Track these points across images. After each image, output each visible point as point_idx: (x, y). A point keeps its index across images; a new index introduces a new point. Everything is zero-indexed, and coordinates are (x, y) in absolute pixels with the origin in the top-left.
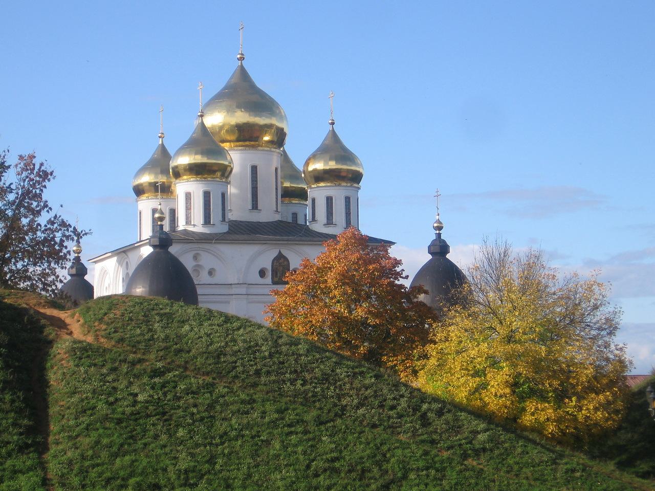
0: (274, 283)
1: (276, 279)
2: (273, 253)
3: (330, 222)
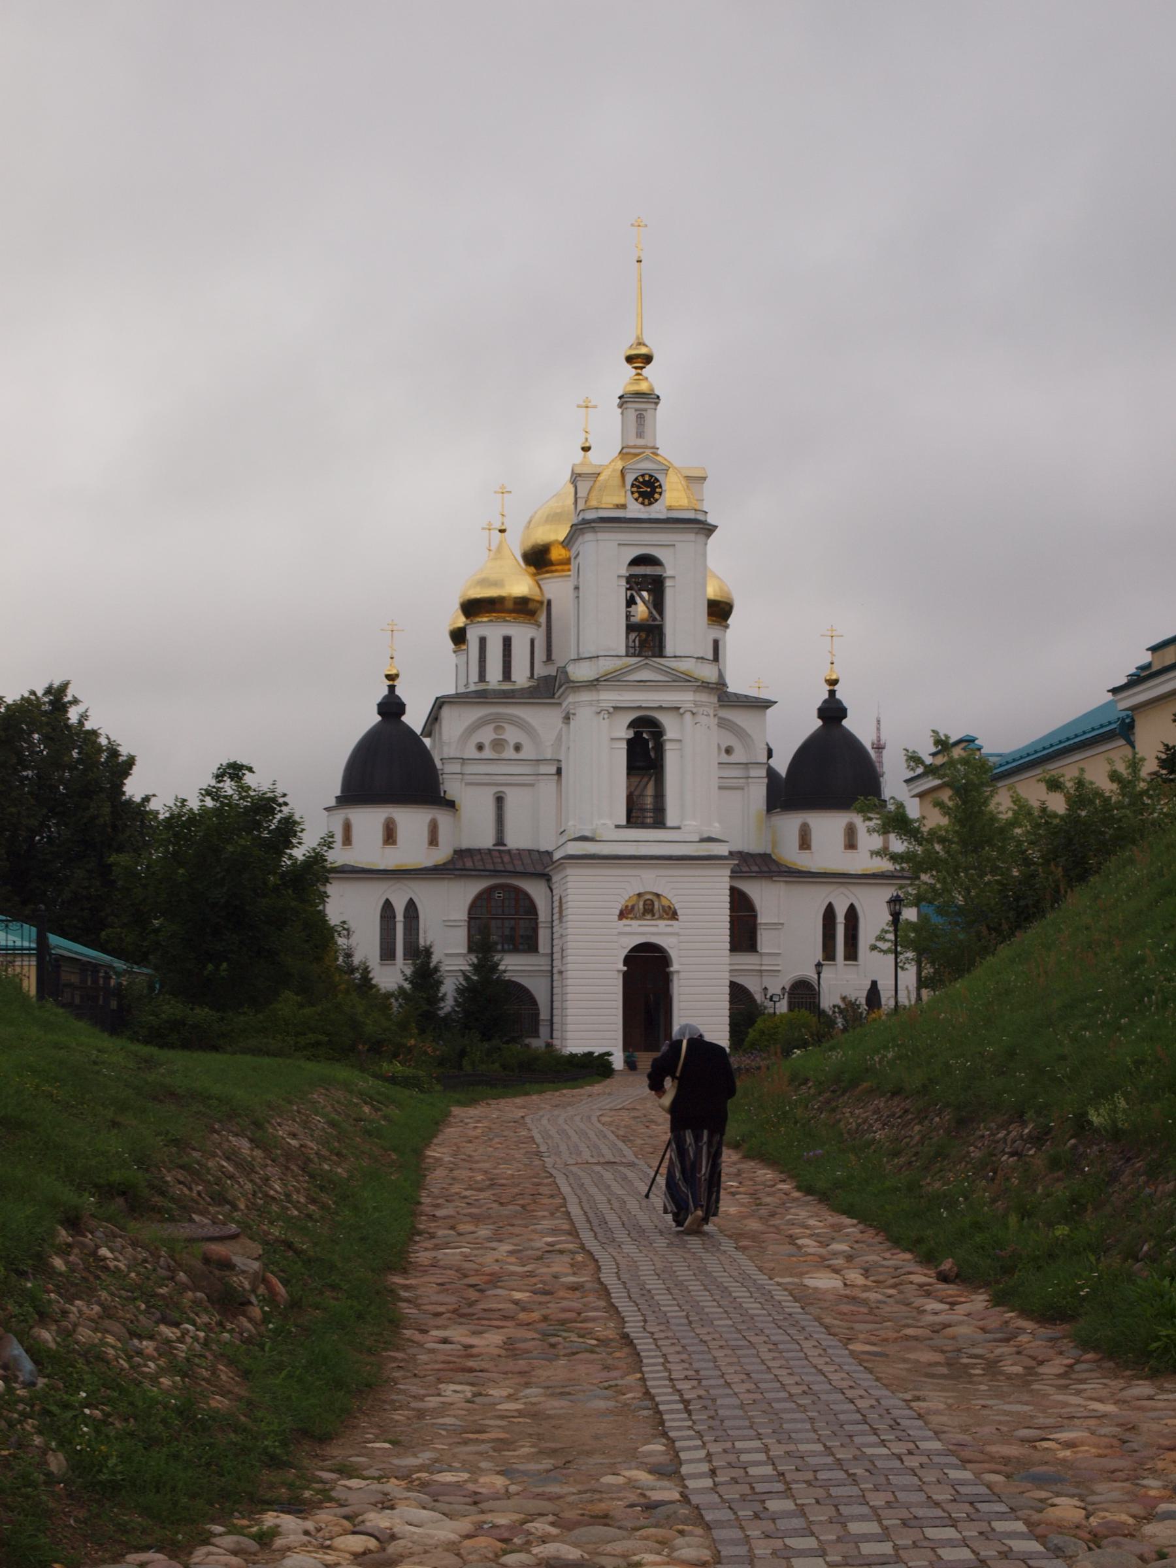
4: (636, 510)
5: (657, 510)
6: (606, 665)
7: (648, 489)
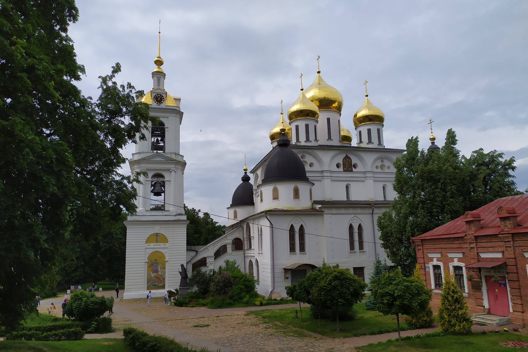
0: (344, 171)
1: (345, 169)
2: (344, 156)
3: (370, 141)
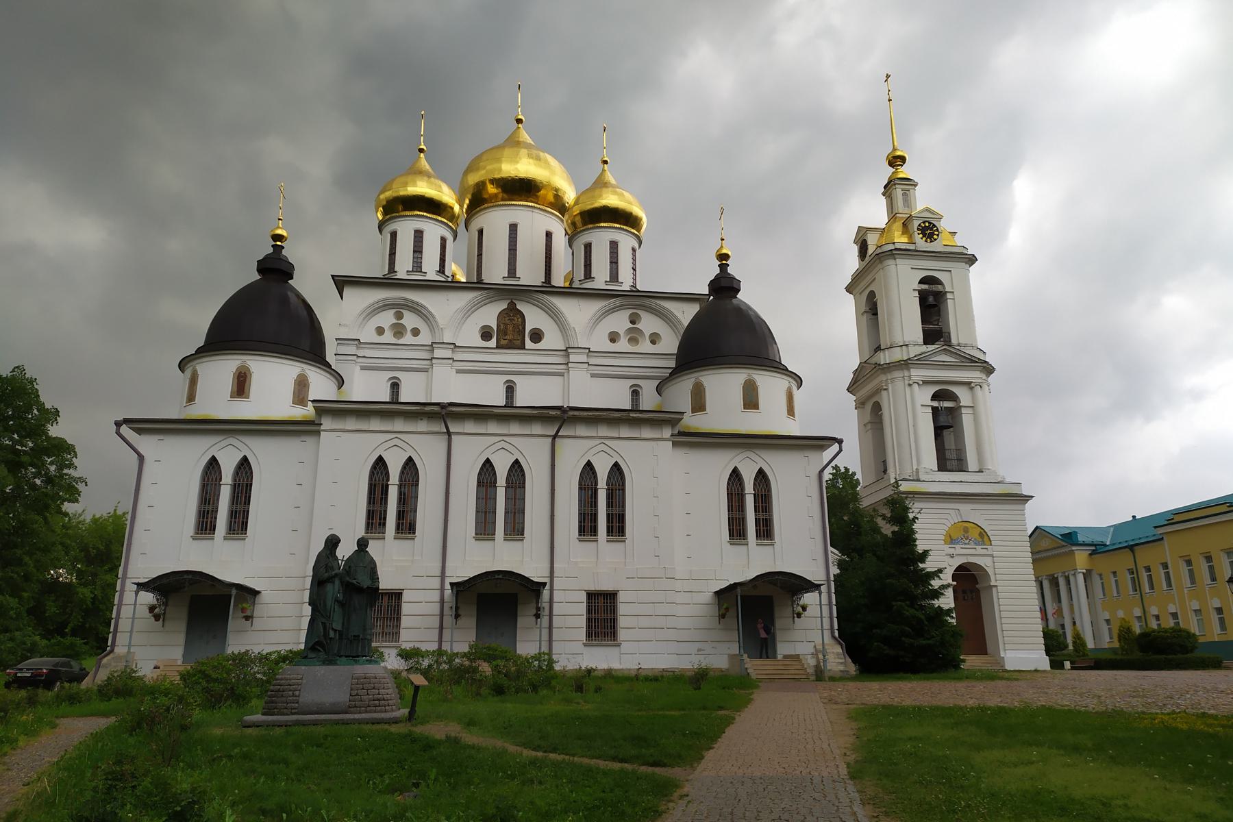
1: (503, 342)
2: (503, 305)
4: (921, 243)
5: (935, 246)
6: (914, 351)
7: (929, 230)
